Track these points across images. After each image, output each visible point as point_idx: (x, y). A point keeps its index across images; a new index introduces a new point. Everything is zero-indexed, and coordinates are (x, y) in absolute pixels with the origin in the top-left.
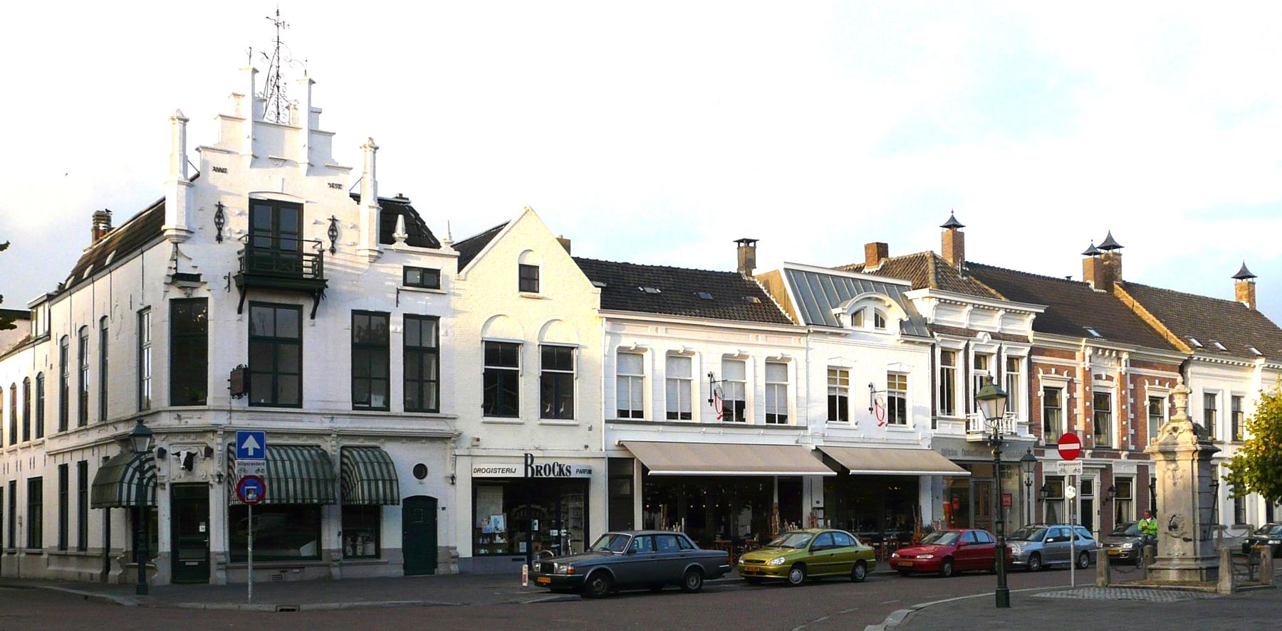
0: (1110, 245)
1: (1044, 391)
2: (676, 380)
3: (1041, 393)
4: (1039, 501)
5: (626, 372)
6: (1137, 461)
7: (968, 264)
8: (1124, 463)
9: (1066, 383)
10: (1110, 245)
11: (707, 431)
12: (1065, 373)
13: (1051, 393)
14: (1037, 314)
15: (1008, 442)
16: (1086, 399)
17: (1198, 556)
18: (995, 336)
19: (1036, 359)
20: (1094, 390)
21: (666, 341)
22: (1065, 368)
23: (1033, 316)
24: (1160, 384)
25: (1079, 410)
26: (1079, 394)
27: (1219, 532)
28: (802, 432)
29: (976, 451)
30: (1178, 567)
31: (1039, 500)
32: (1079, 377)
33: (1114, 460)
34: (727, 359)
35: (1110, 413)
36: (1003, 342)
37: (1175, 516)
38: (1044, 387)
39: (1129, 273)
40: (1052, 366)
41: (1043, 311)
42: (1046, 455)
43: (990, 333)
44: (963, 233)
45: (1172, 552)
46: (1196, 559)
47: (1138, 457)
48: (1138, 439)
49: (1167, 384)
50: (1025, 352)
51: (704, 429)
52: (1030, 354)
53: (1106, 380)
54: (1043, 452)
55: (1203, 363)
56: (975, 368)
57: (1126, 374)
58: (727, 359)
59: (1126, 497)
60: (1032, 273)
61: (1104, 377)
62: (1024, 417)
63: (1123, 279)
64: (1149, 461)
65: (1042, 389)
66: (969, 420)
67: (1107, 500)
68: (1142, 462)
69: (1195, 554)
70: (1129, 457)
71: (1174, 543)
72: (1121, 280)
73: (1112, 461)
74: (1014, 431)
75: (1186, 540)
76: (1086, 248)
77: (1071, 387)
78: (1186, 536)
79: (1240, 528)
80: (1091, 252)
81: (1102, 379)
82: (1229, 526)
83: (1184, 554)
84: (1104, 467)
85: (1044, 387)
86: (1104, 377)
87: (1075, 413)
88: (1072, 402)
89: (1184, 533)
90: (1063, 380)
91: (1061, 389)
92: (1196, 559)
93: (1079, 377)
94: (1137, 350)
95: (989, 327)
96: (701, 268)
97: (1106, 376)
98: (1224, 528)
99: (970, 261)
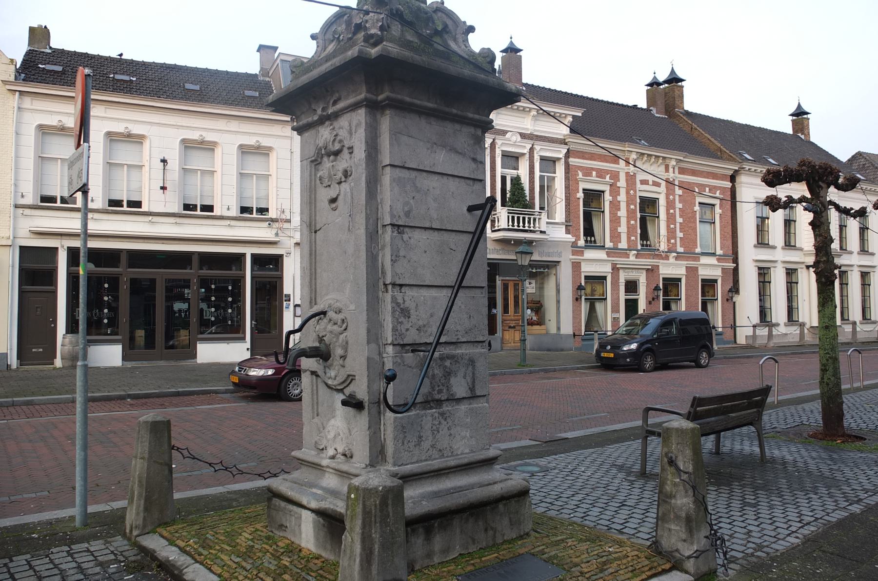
0: (674, 80)
1: (583, 193)
2: (122, 165)
3: (580, 195)
4: (577, 299)
5: (48, 154)
6: (686, 262)
7: (526, 85)
8: (671, 264)
9: (609, 186)
10: (674, 80)
11: (153, 221)
12: (608, 177)
13: (593, 197)
14: (574, 117)
15: (536, 241)
16: (630, 201)
18: (523, 136)
19: (573, 161)
20: (639, 194)
21: (105, 122)
22: (607, 172)
23: (570, 119)
24: (710, 191)
25: (623, 213)
26: (622, 197)
27: (769, 330)
28: (286, 225)
29: (503, 249)
31: (577, 299)
32: (622, 183)
33: (661, 261)
34: (188, 145)
35: (658, 217)
36: (536, 142)
38: (584, 190)
39: (690, 105)
40: (593, 169)
41: (580, 115)
42: (585, 255)
43: (519, 133)
44: (521, 56)
47: (687, 259)
48: (689, 240)
49: (718, 192)
50: (560, 152)
51: (150, 218)
52: (567, 155)
53: (653, 185)
54: (583, 252)
55: (754, 174)
56: (502, 168)
57: (674, 180)
58: (188, 145)
59: (712, 297)
60: (601, 99)
61: (651, 183)
62: (560, 215)
63: (686, 108)
64: (699, 263)
65: (581, 191)
66: (494, 218)
67: (653, 299)
68: (692, 263)
70: (677, 258)
72: (683, 108)
73: (659, 262)
74: (542, 229)
76: (649, 80)
77: (615, 190)
79: (792, 325)
80: (654, 84)
81: (648, 184)
82: (782, 324)
84: (650, 267)
85: (584, 190)
86: (651, 183)
87: (619, 215)
88: (615, 206)
90: (605, 183)
91: (603, 192)
93: (622, 183)
94: (684, 157)
95: (519, 128)
96: (212, 66)
97: (653, 181)
98: (778, 325)
99: (530, 83)
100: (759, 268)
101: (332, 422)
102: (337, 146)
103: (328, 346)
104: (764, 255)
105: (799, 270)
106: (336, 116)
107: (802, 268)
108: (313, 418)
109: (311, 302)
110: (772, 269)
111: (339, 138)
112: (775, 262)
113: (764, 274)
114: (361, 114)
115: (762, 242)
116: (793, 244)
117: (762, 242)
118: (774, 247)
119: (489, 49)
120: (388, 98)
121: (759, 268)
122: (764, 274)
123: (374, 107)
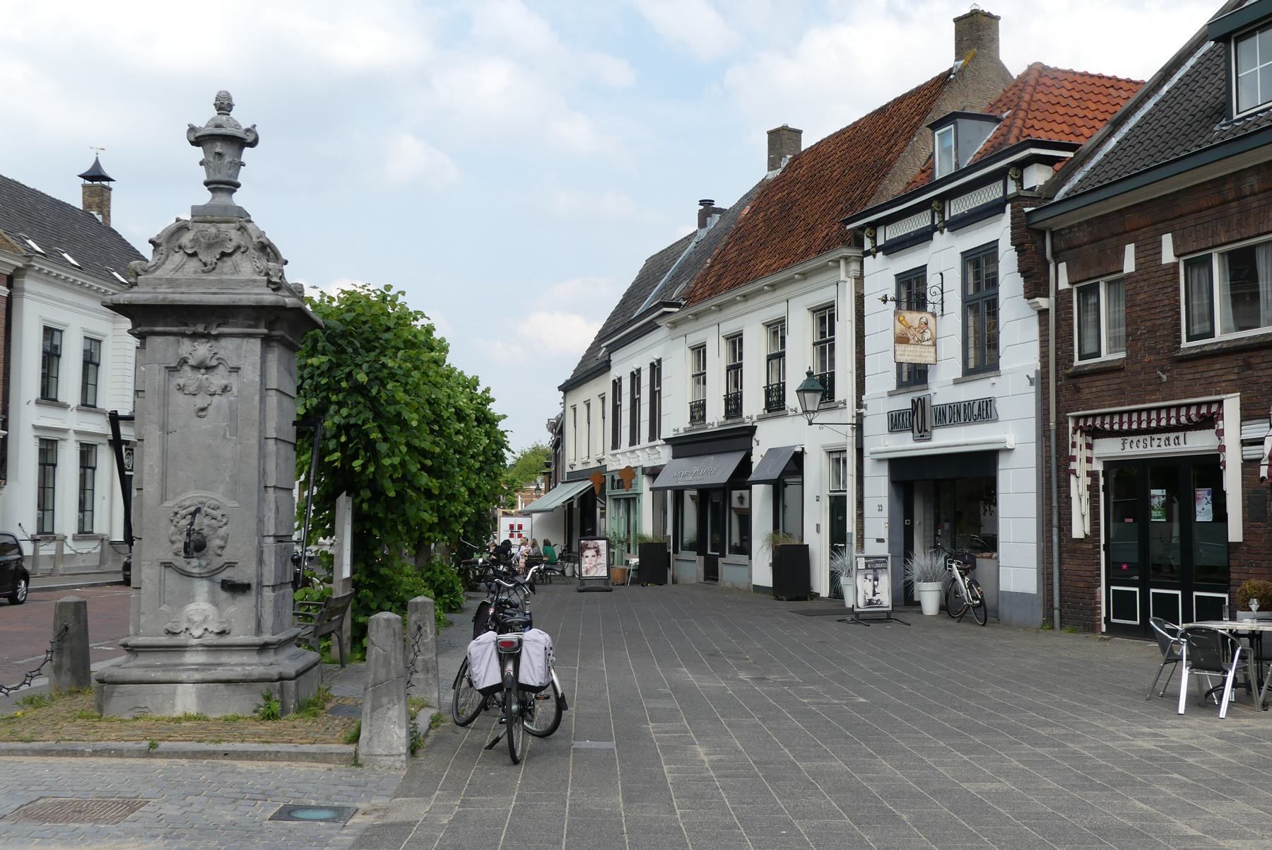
17: (267, 637)
30: (198, 676)
37: (198, 510)
45: (185, 625)
46: (263, 648)
69: (259, 630)
71: (190, 597)
75: (235, 588)
78: (226, 575)
83: (222, 633)
89: (231, 565)
92: (263, 648)
100: (42, 440)
101: (191, 608)
102: (214, 363)
103: (204, 538)
104: (50, 418)
105: (99, 447)
106: (218, 337)
107: (104, 444)
108: (160, 606)
109: (162, 499)
110: (60, 444)
111: (218, 356)
112: (65, 431)
113: (48, 450)
114: (256, 345)
115: (48, 396)
116: (90, 402)
117: (48, 396)
118: (64, 406)
119: (302, 285)
120: (282, 337)
121: (42, 440)
122: (48, 450)
123: (267, 341)
